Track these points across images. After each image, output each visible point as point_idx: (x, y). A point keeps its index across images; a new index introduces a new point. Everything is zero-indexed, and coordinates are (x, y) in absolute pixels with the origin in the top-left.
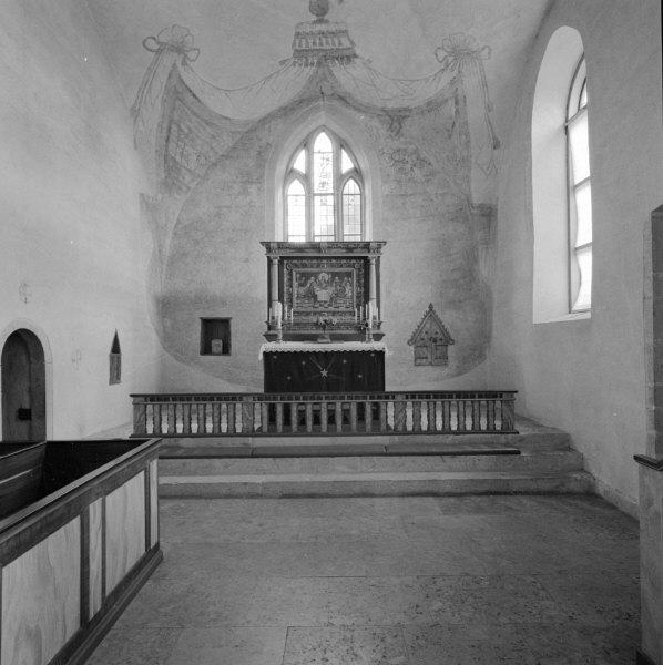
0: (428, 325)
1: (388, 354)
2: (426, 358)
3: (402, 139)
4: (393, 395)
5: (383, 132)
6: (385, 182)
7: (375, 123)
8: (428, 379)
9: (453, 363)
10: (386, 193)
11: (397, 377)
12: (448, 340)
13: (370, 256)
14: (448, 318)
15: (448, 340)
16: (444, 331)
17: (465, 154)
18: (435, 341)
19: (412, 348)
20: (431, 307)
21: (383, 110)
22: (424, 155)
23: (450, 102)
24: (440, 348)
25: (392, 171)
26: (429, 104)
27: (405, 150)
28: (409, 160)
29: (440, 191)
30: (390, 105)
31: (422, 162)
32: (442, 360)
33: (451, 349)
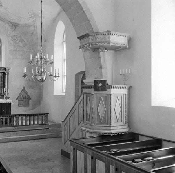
0: (23, 94)
1: (12, 104)
2: (22, 104)
3: (16, 32)
4: (14, 116)
5: (10, 29)
6: (10, 46)
7: (7, 25)
8: (22, 111)
9: (31, 106)
10: (9, 50)
11: (15, 111)
12: (29, 98)
13: (6, 72)
14: (29, 91)
15: (29, 98)
16: (28, 96)
17: (36, 42)
18: (25, 99)
19: (18, 101)
20: (24, 88)
21: (10, 22)
22: (23, 38)
23: (32, 26)
24: (26, 101)
25: (12, 42)
26: (26, 25)
27: (16, 36)
28: (18, 39)
29: (28, 51)
30: (13, 21)
31: (22, 40)
32: (27, 105)
33: (30, 101)
